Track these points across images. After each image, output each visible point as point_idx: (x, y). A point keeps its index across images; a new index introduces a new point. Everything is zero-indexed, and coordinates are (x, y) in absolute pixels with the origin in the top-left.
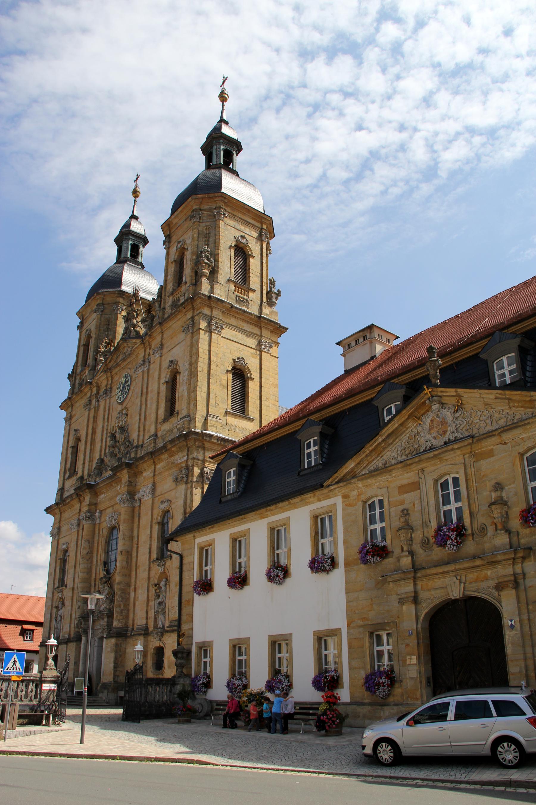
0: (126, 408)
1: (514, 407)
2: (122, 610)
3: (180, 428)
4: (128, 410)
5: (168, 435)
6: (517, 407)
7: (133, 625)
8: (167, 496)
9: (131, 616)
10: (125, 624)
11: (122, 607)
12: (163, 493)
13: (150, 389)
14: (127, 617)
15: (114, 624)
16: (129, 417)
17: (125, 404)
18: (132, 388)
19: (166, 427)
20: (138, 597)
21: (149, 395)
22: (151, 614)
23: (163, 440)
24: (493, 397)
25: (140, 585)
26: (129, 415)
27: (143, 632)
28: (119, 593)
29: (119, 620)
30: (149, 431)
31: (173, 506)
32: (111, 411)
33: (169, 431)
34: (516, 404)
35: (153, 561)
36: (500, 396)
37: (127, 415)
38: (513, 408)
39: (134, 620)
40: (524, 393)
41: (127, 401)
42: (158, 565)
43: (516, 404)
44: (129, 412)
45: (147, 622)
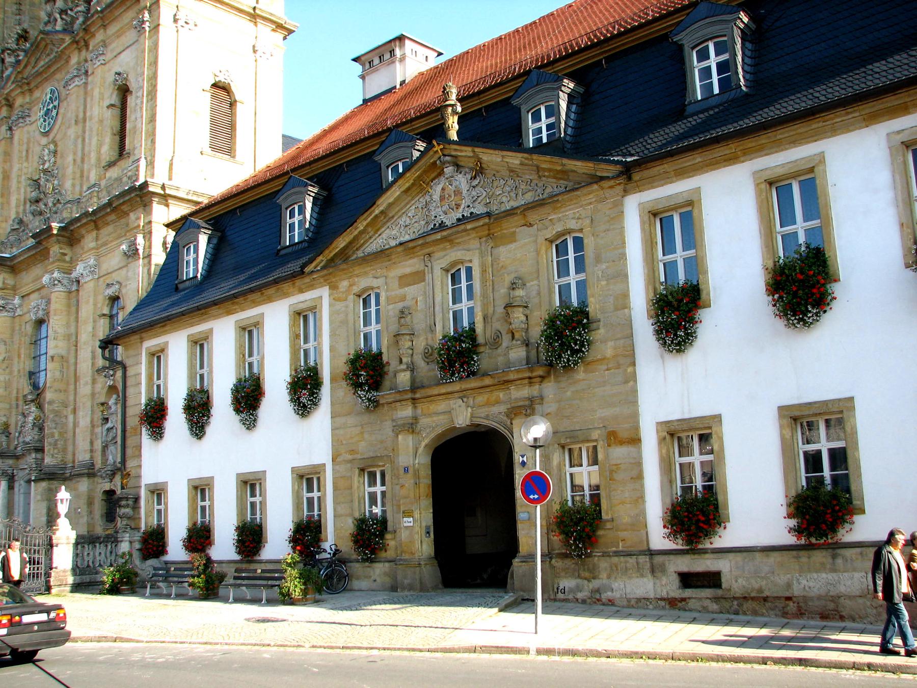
0: (54, 142)
1: (544, 176)
2: (57, 441)
3: (132, 176)
4: (56, 145)
5: (115, 186)
6: (548, 177)
7: (74, 462)
8: (116, 277)
9: (70, 449)
10: (62, 461)
11: (57, 436)
12: (109, 271)
13: (88, 114)
14: (64, 450)
15: (46, 461)
16: (58, 156)
17: (52, 136)
18: (62, 111)
19: (113, 173)
20: (78, 422)
21: (88, 124)
22: (98, 445)
23: (109, 192)
24: (517, 162)
25: (81, 404)
26: (58, 152)
27: (86, 471)
28: (51, 416)
29: (53, 455)
30: (88, 178)
31: (124, 291)
32: (31, 145)
33: (116, 179)
34: (546, 174)
35: (98, 371)
36: (526, 161)
37: (55, 152)
38: (544, 179)
39: (74, 455)
40: (556, 159)
41: (55, 131)
42: (105, 376)
43: (546, 174)
44: (59, 149)
45: (92, 457)
